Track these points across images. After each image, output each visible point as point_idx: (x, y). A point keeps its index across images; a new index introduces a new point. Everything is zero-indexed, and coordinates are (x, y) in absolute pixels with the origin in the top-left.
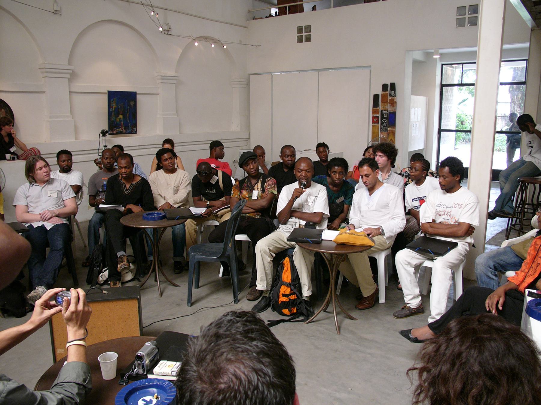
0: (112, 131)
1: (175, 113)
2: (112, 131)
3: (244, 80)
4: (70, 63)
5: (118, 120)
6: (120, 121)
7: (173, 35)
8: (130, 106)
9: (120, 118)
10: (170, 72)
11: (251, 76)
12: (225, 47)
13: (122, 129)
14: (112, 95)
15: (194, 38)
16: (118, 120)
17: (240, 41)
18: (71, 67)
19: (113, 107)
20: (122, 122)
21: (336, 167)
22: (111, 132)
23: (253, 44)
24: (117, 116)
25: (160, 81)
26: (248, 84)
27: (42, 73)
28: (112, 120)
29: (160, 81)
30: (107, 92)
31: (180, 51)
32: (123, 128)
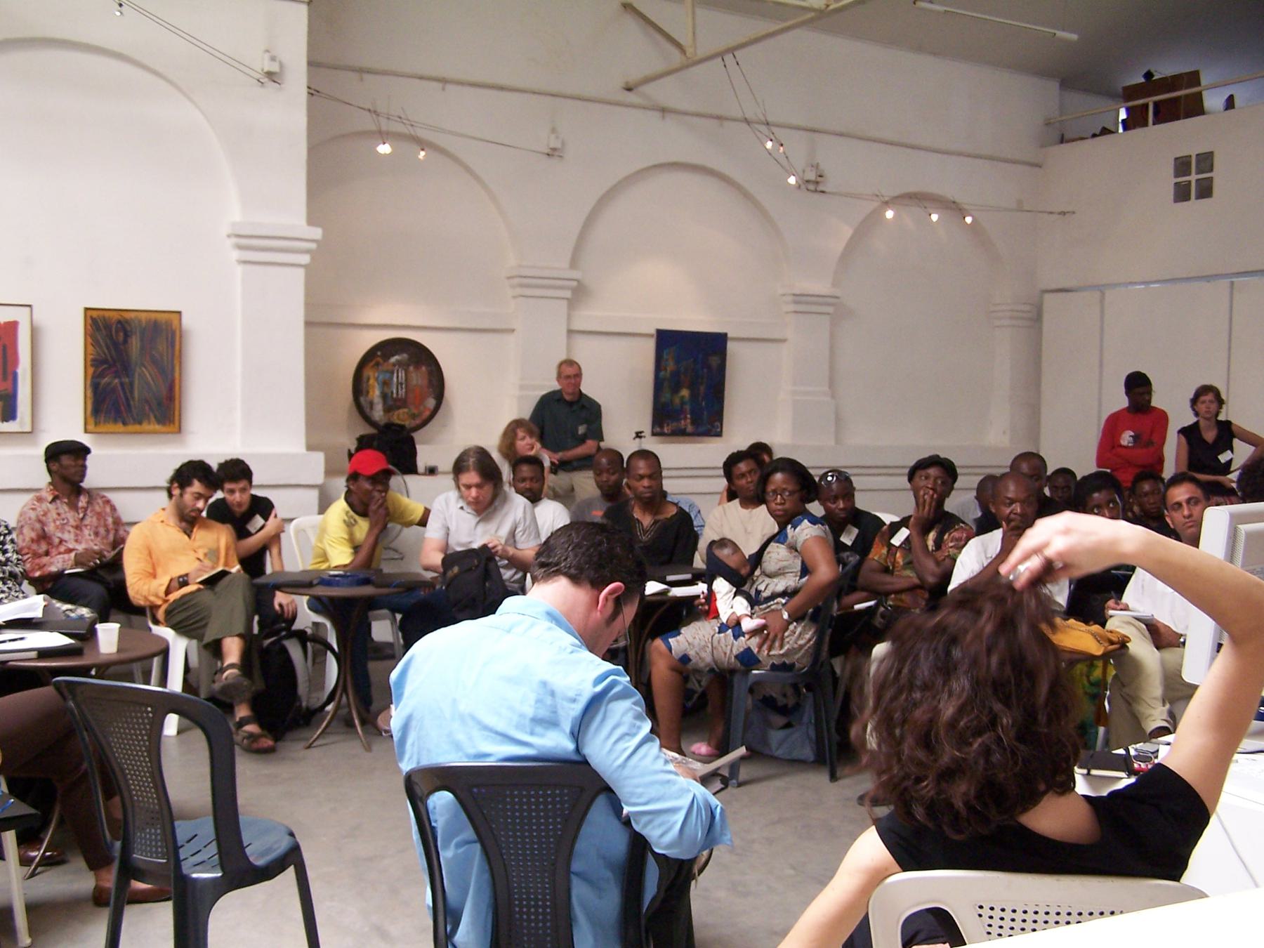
0: (661, 427)
1: (828, 389)
2: (661, 427)
3: (1027, 308)
4: (574, 264)
5: (677, 401)
6: (683, 403)
7: (829, 193)
8: (709, 367)
9: (683, 397)
10: (820, 286)
11: (1047, 296)
12: (969, 220)
13: (687, 424)
14: (667, 340)
15: (886, 199)
16: (677, 401)
17: (1020, 202)
18: (575, 274)
19: (666, 369)
20: (688, 407)
21: (1096, 495)
22: (658, 429)
23: (1053, 211)
24: (676, 389)
25: (792, 307)
26: (1036, 318)
27: (513, 287)
28: (663, 400)
29: (792, 307)
30: (653, 331)
31: (847, 232)
32: (689, 421)
